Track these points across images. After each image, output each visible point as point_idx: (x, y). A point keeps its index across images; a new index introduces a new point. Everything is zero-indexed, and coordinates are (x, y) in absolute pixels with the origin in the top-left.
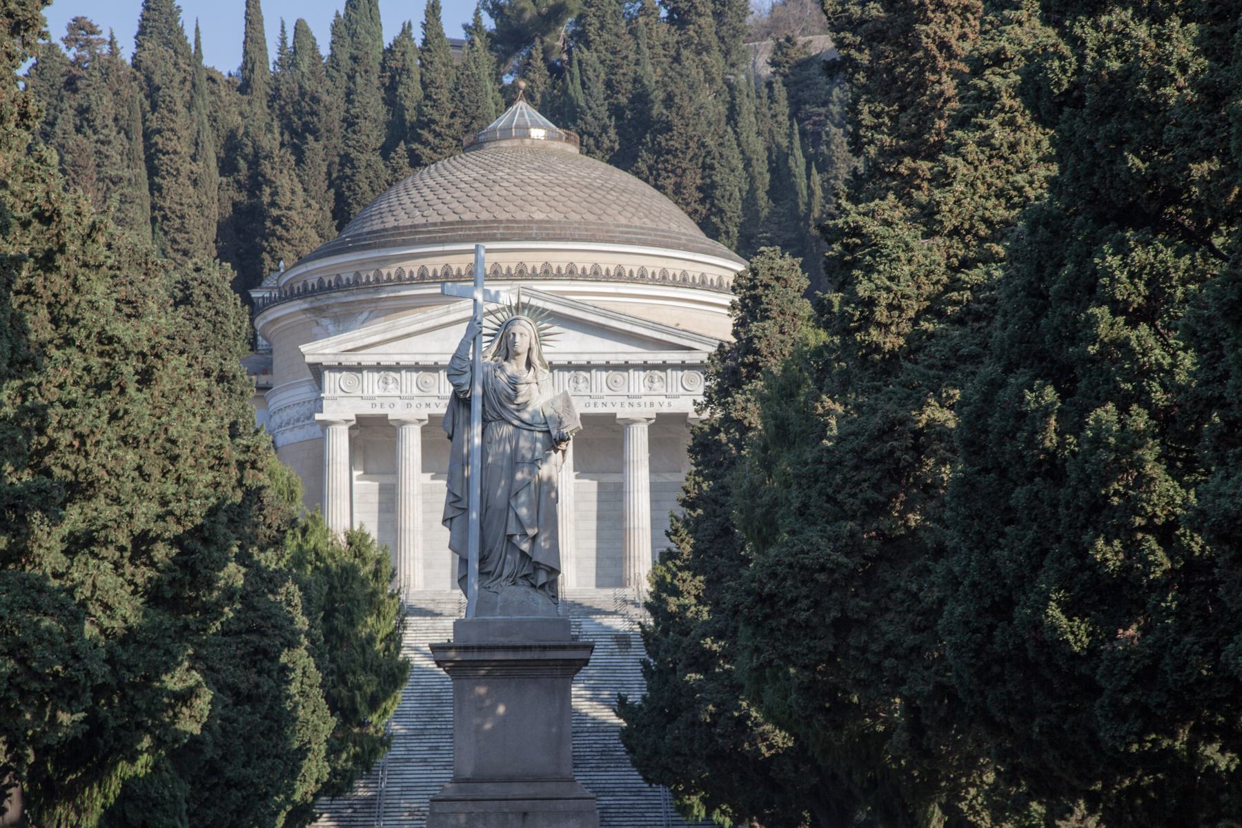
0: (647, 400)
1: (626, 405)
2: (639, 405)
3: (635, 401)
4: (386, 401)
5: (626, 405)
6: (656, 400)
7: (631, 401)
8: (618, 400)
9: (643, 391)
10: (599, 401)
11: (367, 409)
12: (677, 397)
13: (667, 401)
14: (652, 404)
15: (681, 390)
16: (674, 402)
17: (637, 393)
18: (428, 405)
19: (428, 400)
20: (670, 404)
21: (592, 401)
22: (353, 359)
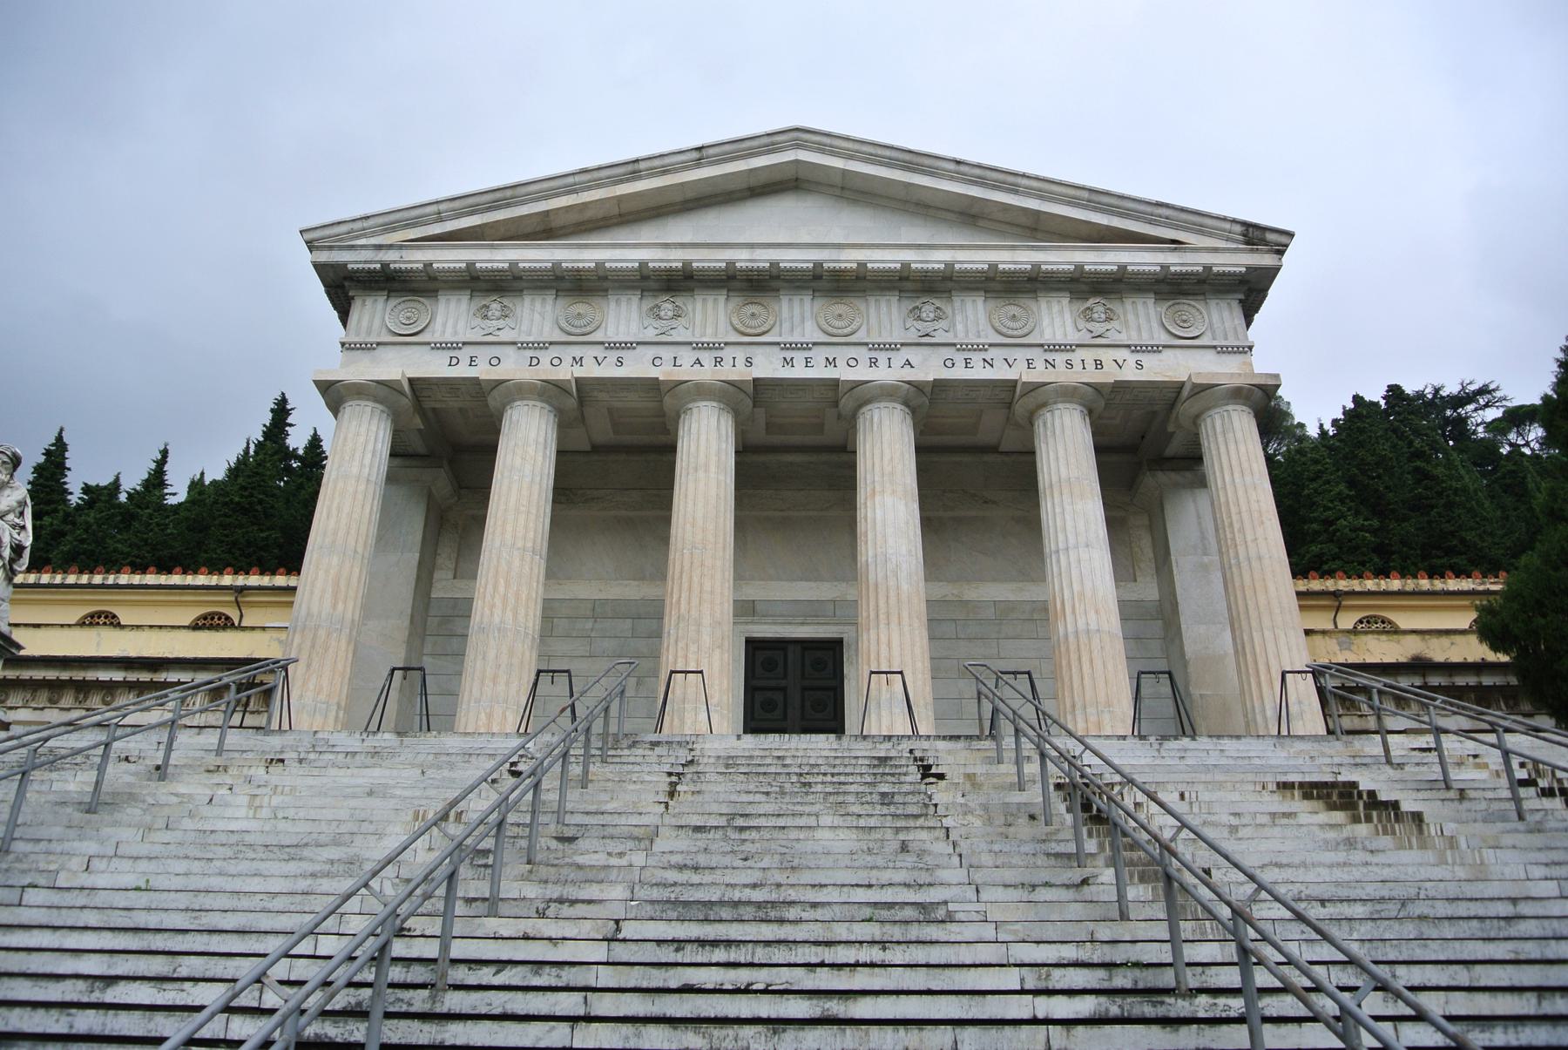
0: (1089, 355)
1: (1039, 365)
2: (1069, 364)
3: (1060, 358)
4: (484, 354)
5: (1039, 365)
6: (1107, 356)
7: (1050, 356)
8: (1021, 355)
9: (1073, 337)
10: (976, 358)
11: (434, 366)
12: (1155, 349)
13: (1132, 359)
14: (1098, 364)
15: (1164, 339)
16: (1147, 359)
17: (1059, 339)
18: (578, 361)
19: (577, 351)
20: (1139, 365)
21: (959, 358)
22: (415, 259)
